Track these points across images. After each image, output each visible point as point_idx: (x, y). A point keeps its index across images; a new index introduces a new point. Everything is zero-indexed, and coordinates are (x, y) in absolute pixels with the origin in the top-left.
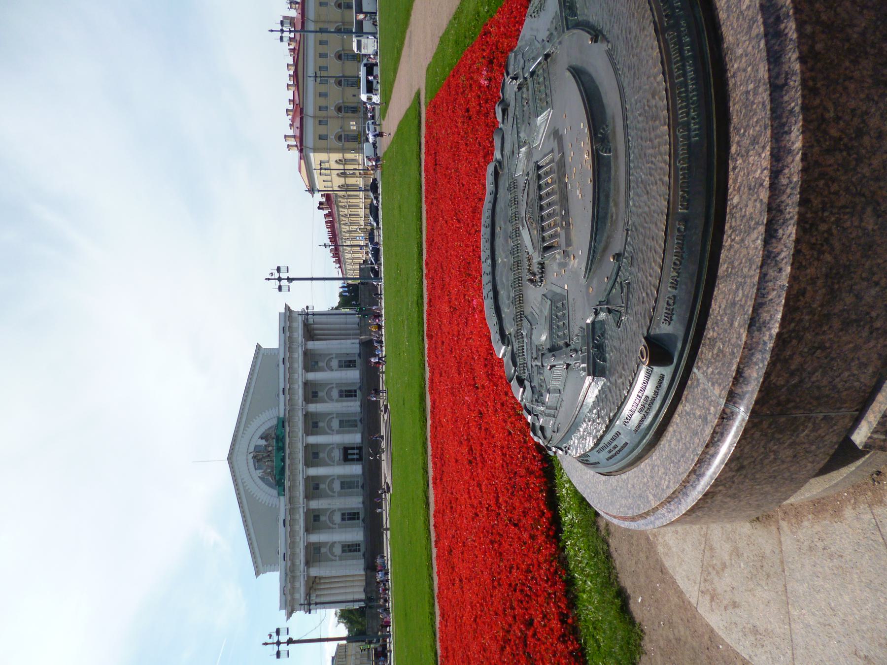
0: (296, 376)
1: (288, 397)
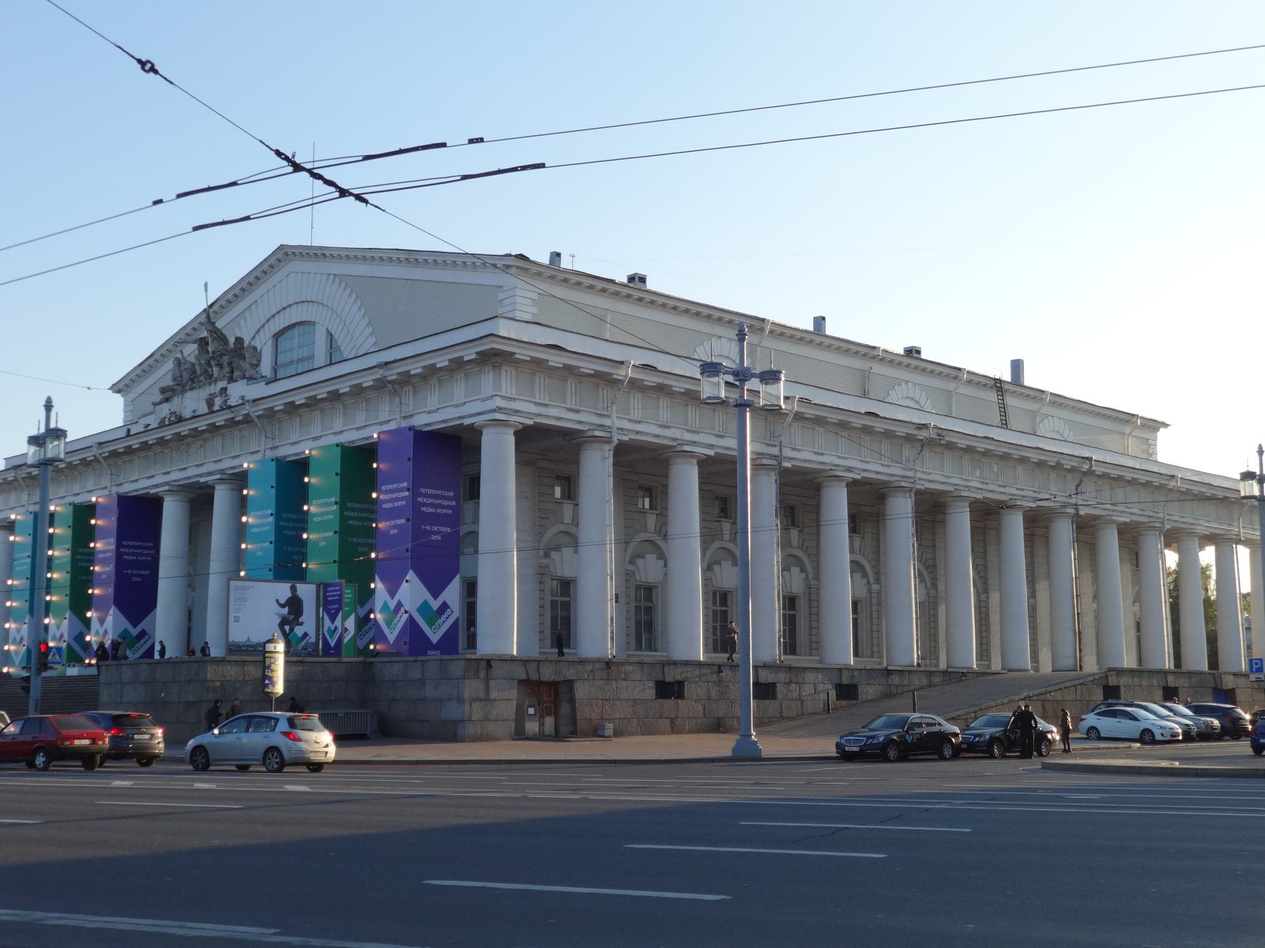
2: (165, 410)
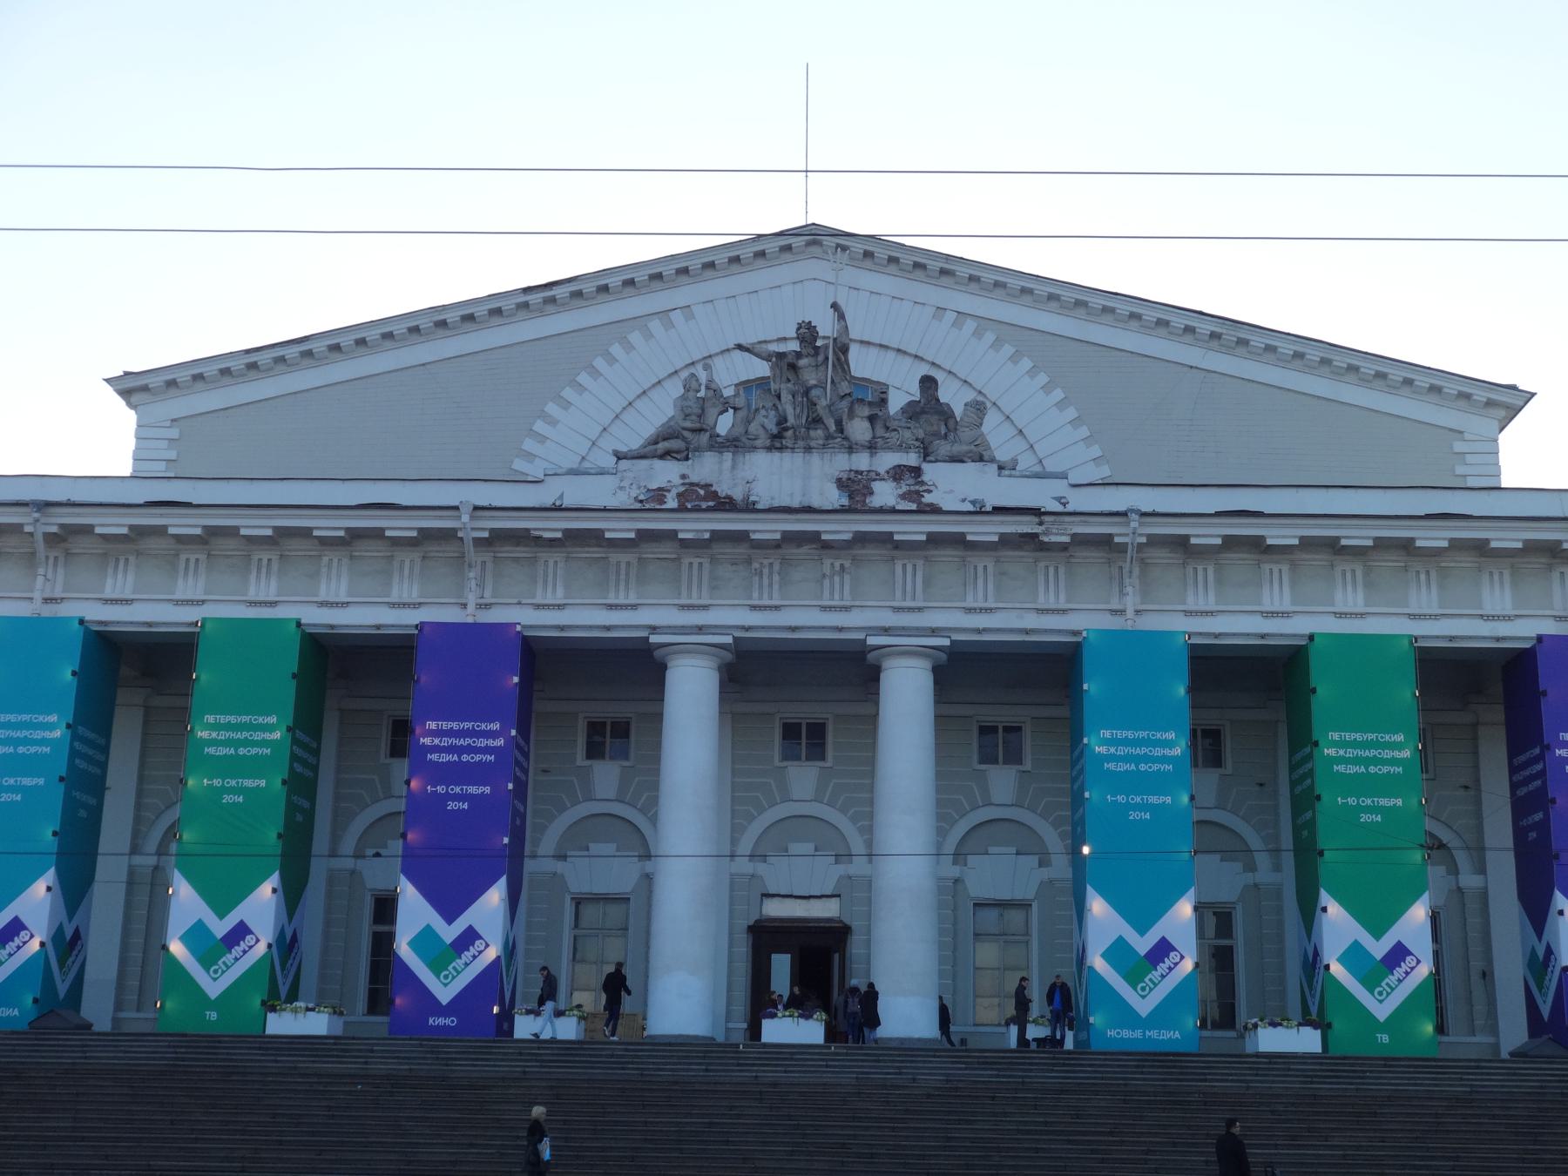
0: (1351, 597)
1: (1207, 535)
2: (667, 474)
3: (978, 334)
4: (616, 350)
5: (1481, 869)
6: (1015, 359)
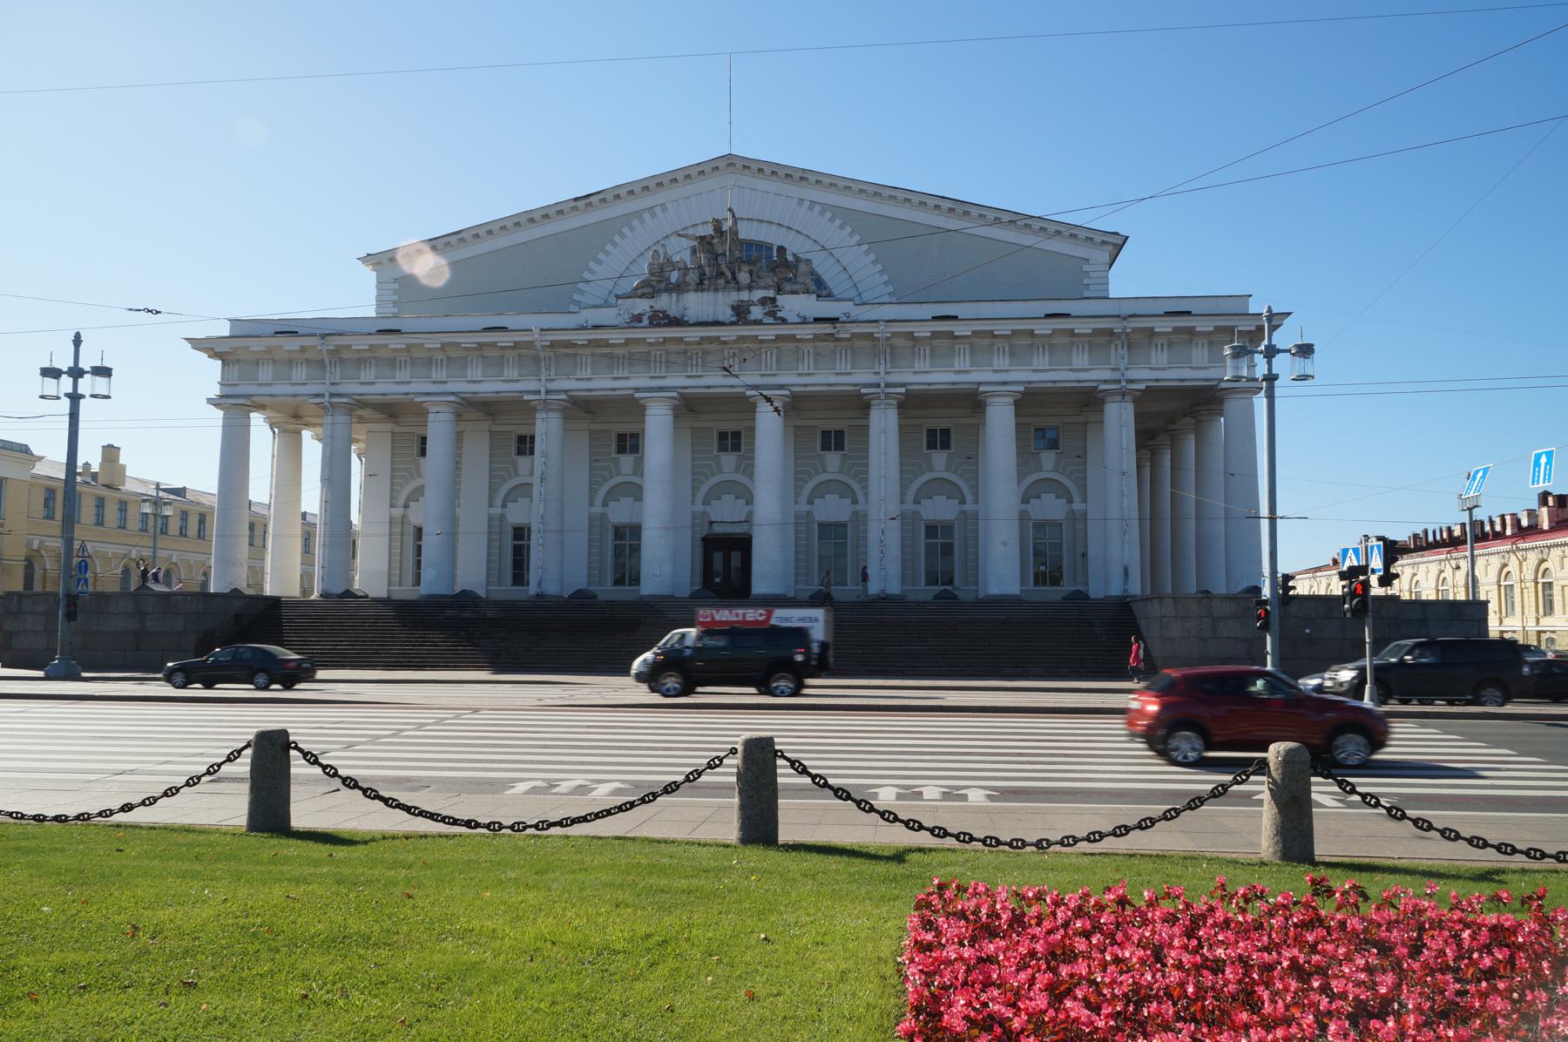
0: (1002, 362)
2: (643, 306)
3: (822, 213)
4: (626, 231)
5: (1085, 501)
6: (842, 227)
